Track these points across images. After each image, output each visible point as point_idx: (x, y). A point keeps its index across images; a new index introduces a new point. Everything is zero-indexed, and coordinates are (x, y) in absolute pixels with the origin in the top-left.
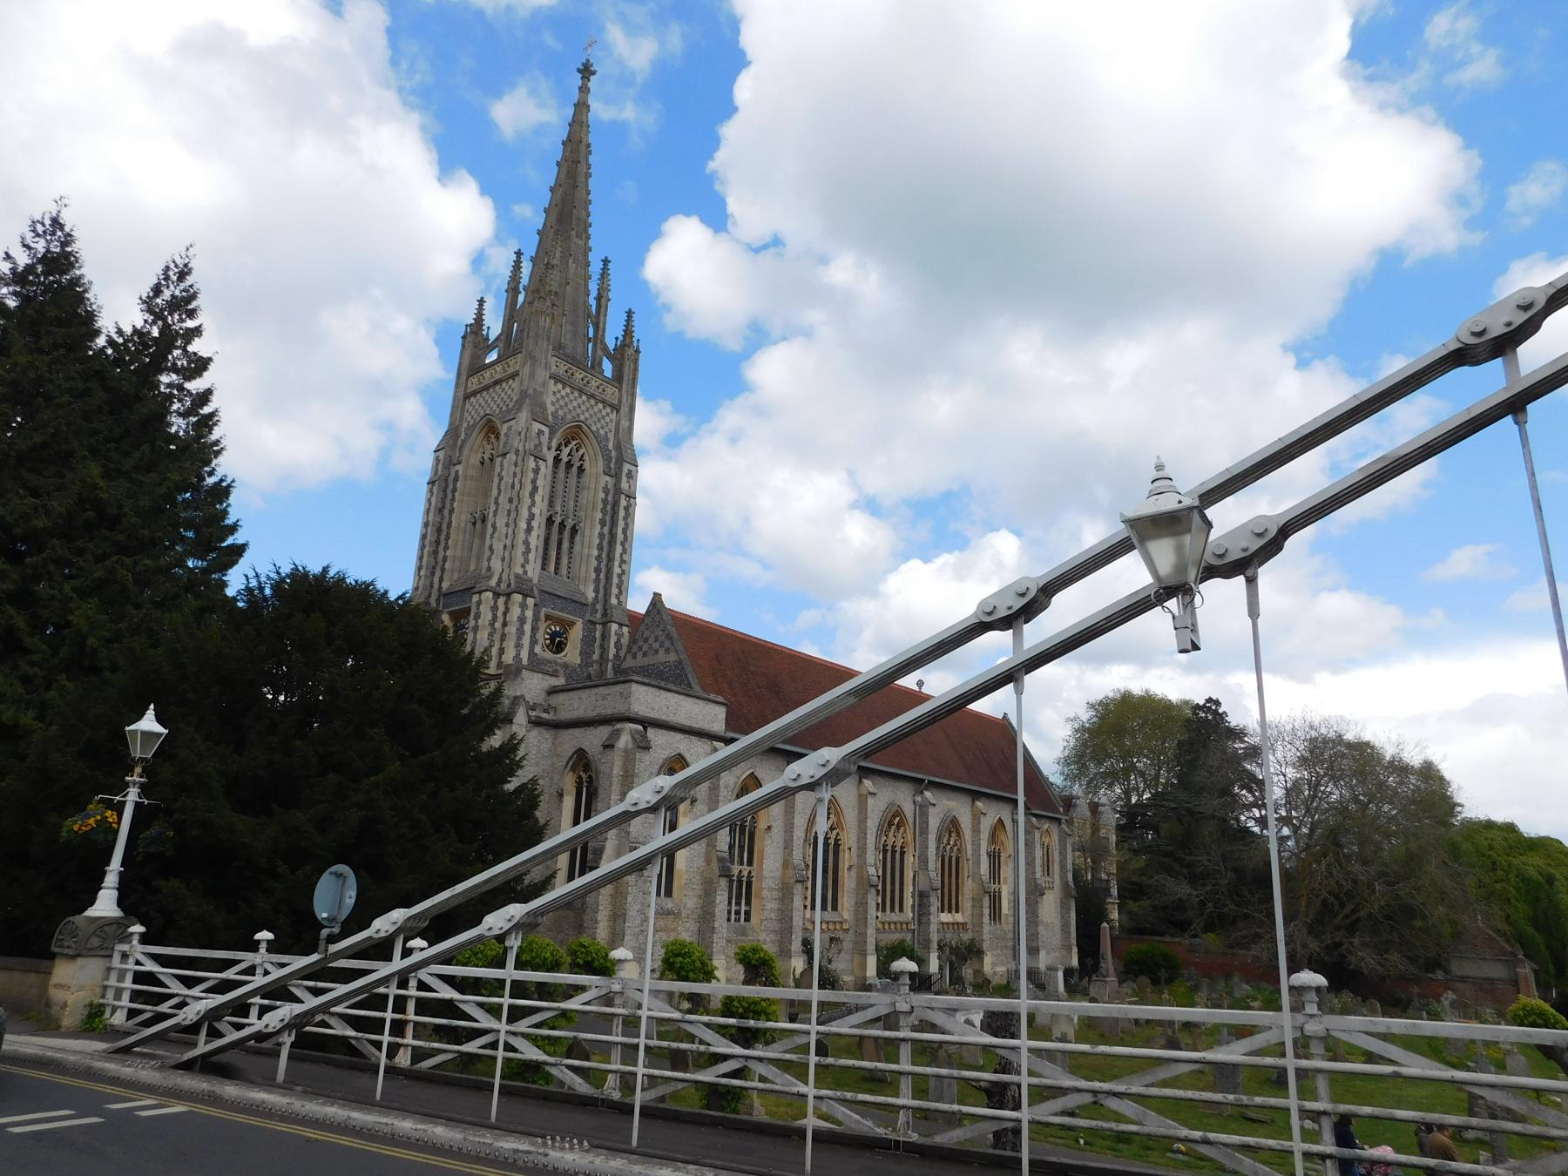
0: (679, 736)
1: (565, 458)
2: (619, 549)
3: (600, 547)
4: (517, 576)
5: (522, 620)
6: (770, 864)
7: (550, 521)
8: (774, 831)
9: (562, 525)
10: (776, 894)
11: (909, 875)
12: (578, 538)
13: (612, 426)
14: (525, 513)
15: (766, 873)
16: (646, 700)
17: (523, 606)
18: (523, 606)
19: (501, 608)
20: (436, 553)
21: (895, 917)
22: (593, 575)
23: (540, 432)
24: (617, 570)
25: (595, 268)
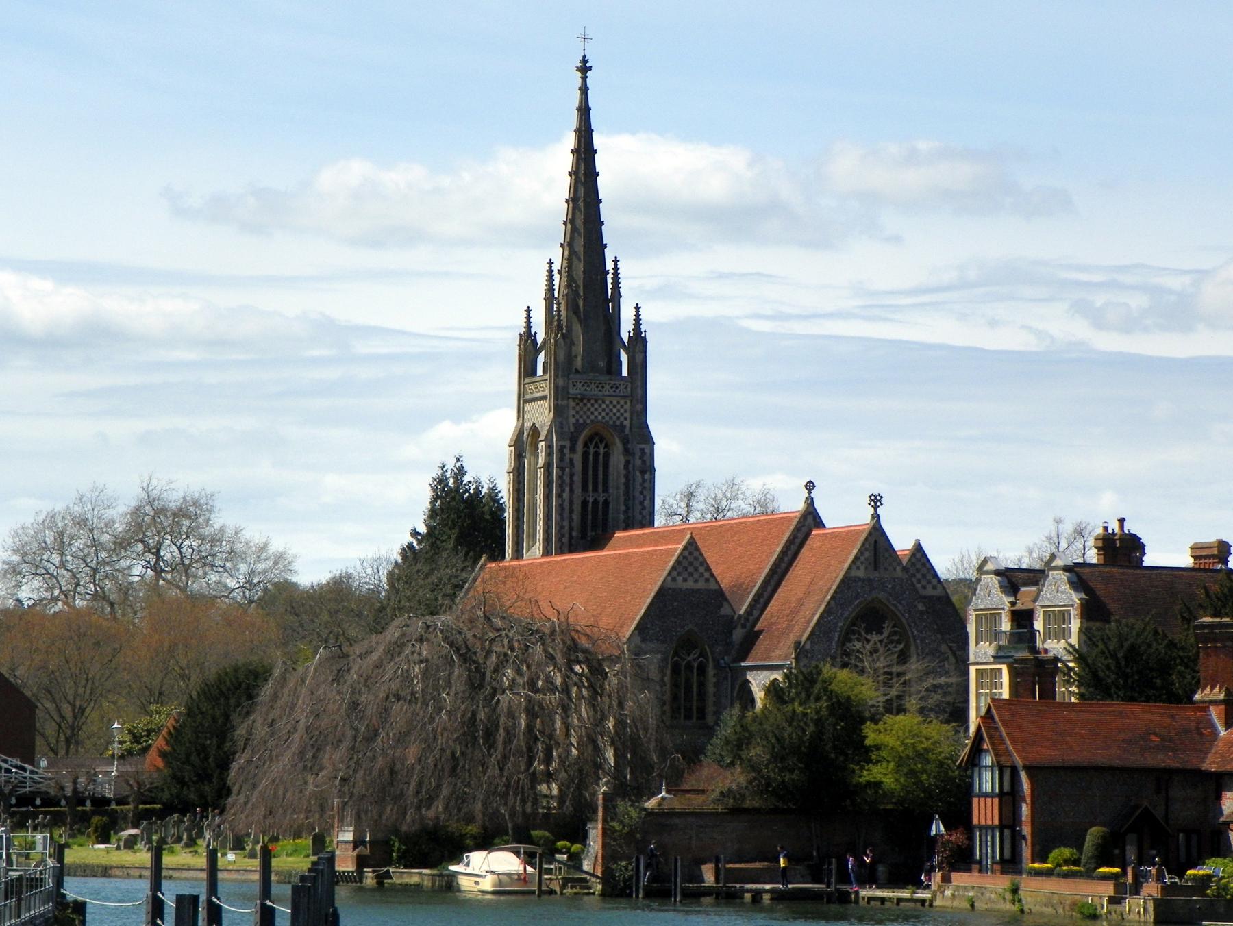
9: (596, 502)
13: (627, 415)
25: (610, 266)
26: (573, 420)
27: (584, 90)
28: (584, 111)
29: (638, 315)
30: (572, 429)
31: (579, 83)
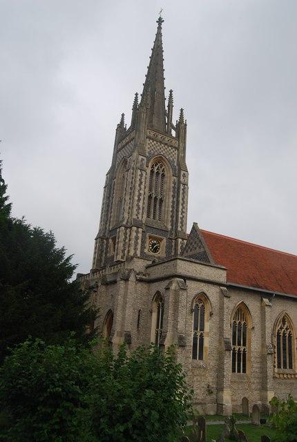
0: (202, 284)
2: (181, 207)
3: (173, 207)
5: (137, 238)
6: (254, 345)
7: (150, 197)
8: (256, 330)
9: (156, 198)
10: (258, 360)
12: (163, 204)
14: (137, 193)
15: (252, 350)
16: (184, 267)
17: (137, 232)
18: (137, 232)
19: (128, 234)
20: (107, 215)
22: (170, 219)
24: (180, 216)
25: (167, 94)
26: (148, 150)
28: (159, 35)
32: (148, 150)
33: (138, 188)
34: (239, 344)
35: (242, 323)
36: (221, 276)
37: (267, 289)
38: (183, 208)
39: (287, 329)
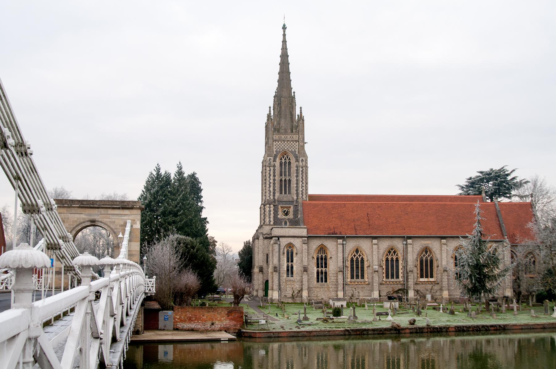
0: (290, 238)
1: (283, 161)
2: (301, 183)
3: (297, 184)
4: (268, 200)
5: (270, 211)
6: (332, 267)
7: (281, 180)
9: (285, 180)
11: (400, 267)
13: (297, 147)
14: (268, 183)
17: (270, 207)
18: (270, 207)
21: (398, 280)
22: (295, 192)
23: (270, 159)
24: (301, 189)
26: (275, 150)
27: (284, 35)
28: (284, 42)
29: (301, 111)
30: (275, 153)
31: (282, 33)
32: (275, 150)
33: (268, 179)
34: (322, 267)
35: (324, 255)
36: (304, 232)
37: (341, 233)
38: (303, 183)
39: (360, 256)
